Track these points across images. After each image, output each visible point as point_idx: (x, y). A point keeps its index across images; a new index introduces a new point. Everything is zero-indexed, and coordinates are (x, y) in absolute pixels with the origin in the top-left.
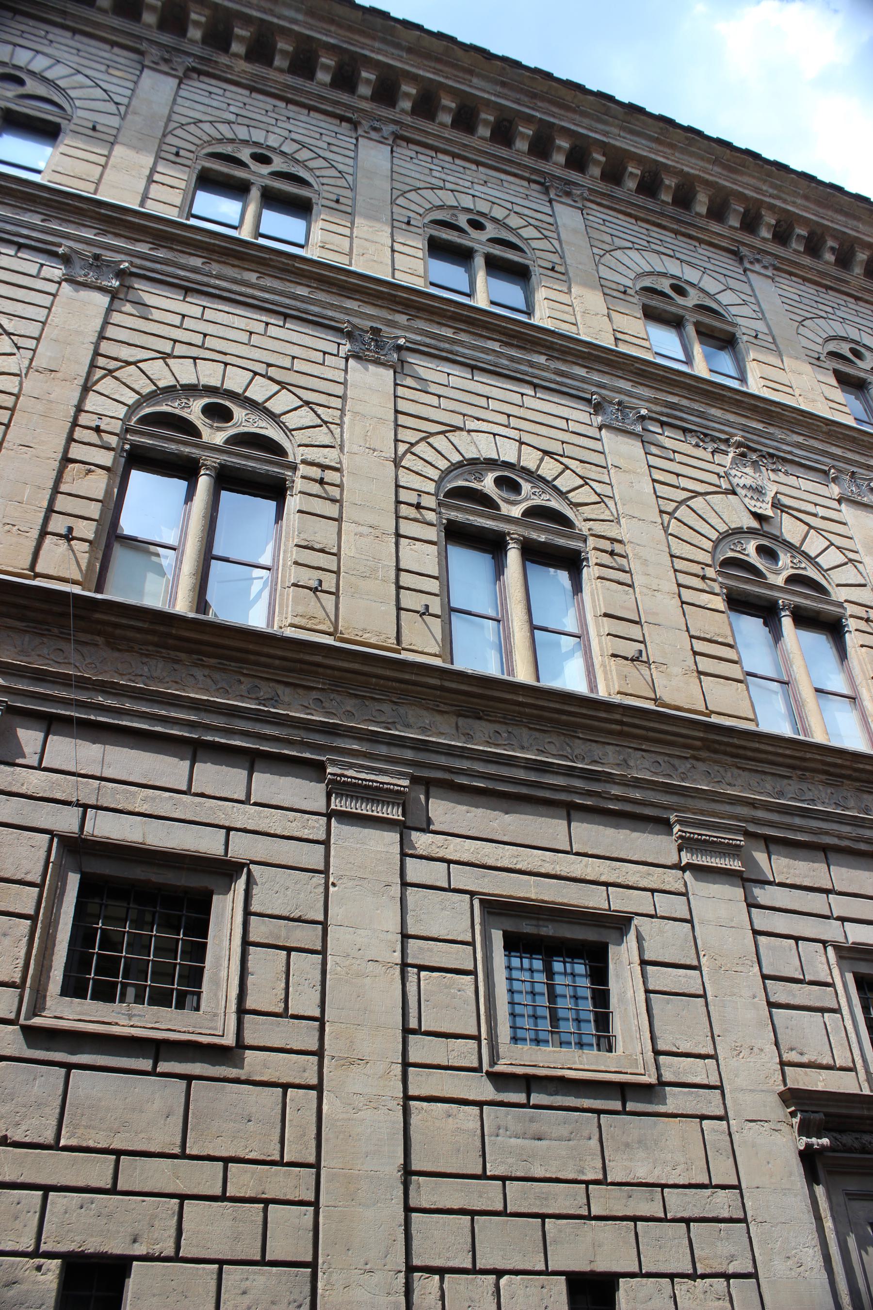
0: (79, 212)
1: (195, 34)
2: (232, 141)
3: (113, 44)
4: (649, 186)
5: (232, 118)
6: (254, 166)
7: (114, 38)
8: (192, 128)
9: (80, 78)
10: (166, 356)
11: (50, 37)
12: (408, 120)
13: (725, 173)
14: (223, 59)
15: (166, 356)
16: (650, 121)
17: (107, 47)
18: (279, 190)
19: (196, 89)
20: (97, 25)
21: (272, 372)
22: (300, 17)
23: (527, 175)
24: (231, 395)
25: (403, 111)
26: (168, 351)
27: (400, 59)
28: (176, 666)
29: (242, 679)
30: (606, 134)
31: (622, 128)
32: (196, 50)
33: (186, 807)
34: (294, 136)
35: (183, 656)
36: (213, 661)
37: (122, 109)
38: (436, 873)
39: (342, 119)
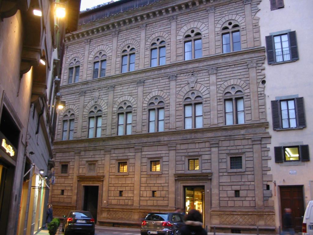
12: (147, 21)
20: (106, 34)
30: (175, 3)
33: (125, 154)
38: (144, 156)
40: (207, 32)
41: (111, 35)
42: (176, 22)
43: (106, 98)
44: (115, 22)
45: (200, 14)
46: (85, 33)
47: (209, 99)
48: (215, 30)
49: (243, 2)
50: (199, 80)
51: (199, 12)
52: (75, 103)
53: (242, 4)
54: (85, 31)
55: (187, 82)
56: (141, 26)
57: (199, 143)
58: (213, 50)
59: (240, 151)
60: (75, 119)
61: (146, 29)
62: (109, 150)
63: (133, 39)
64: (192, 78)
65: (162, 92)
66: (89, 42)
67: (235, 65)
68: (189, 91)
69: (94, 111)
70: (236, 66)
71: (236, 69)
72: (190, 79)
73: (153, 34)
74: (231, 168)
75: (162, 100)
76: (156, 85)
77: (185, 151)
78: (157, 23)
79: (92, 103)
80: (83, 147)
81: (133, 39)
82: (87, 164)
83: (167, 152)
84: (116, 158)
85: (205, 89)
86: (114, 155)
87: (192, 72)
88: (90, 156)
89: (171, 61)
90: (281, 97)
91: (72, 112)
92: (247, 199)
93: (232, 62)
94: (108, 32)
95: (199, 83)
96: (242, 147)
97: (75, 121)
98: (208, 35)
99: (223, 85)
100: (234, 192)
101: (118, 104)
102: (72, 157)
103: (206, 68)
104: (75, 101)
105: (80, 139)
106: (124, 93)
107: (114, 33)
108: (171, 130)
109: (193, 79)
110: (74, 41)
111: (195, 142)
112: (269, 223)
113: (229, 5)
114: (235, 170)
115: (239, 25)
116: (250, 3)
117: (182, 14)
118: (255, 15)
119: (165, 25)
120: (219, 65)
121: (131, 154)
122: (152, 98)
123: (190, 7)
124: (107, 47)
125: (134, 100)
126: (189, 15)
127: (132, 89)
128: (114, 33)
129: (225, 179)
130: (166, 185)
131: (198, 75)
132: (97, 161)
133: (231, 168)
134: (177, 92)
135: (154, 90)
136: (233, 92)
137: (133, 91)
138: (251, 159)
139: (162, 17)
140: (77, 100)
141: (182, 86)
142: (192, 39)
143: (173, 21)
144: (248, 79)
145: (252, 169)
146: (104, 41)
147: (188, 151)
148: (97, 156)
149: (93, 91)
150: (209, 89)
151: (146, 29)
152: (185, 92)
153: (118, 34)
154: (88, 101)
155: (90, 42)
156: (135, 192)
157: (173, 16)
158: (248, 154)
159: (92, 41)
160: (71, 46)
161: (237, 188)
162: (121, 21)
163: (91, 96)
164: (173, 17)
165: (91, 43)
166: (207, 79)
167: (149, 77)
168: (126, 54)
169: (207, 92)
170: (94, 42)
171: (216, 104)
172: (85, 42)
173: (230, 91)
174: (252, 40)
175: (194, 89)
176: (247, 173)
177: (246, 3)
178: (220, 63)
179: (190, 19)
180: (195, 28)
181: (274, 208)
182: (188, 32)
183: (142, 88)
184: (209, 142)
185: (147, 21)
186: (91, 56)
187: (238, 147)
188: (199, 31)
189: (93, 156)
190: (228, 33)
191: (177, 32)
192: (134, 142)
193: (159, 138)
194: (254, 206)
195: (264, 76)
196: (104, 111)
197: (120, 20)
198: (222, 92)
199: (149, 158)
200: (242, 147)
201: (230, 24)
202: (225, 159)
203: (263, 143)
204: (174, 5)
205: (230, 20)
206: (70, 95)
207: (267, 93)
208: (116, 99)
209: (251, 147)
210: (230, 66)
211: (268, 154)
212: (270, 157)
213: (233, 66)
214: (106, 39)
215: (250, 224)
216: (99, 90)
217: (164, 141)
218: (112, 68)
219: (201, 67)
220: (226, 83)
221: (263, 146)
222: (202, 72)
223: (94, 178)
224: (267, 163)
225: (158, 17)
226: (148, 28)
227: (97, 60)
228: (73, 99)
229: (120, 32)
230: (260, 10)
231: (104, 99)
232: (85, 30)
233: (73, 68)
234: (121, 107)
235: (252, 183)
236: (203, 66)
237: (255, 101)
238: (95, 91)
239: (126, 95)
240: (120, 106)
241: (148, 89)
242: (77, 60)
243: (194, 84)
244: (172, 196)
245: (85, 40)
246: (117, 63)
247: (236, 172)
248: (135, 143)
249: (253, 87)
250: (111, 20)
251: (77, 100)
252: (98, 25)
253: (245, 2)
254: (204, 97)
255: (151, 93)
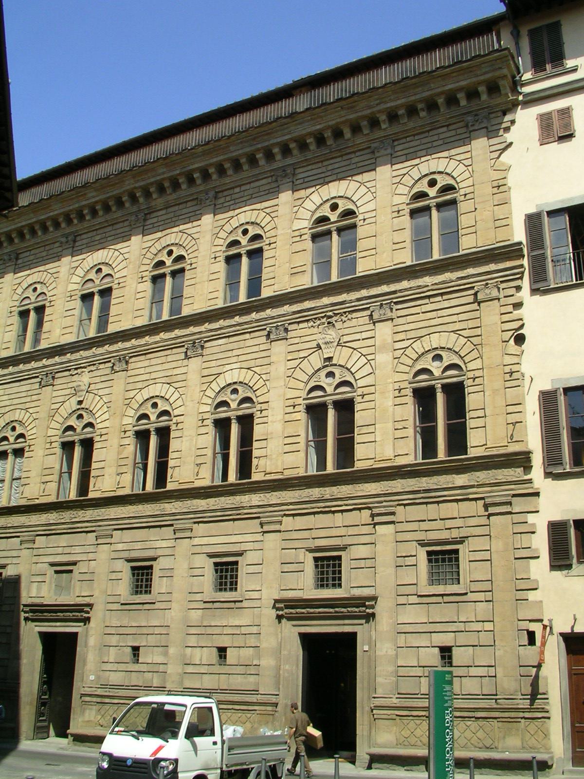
4: (320, 140)
13: (349, 111)
16: (303, 114)
23: (269, 175)
31: (296, 125)
33: (148, 545)
40: (371, 206)
41: (126, 223)
42: (293, 182)
43: (107, 391)
44: (135, 188)
45: (356, 160)
46: (61, 220)
47: (372, 389)
48: (392, 201)
49: (467, 126)
50: (346, 339)
51: (353, 156)
52: (28, 405)
53: (464, 130)
54: (61, 214)
55: (314, 344)
56: (202, 196)
57: (342, 511)
58: (385, 255)
59: (455, 534)
60: (27, 449)
61: (215, 205)
62: (109, 532)
63: (180, 231)
64: (330, 332)
65: (251, 373)
66: (72, 243)
67: (442, 294)
68: (319, 370)
69: (75, 427)
70: (445, 297)
71: (446, 304)
72: (324, 336)
73: (233, 217)
74: (431, 582)
75: (249, 395)
76: (235, 353)
77: (306, 534)
78: (243, 188)
79: (72, 404)
80: (42, 525)
81: (180, 231)
83: (259, 537)
84: (126, 555)
85: (363, 360)
86: (120, 547)
87: (330, 317)
88: (60, 550)
89: (276, 287)
90: (568, 379)
91: (19, 430)
92: (473, 671)
93: (436, 287)
94: (119, 214)
95: (347, 344)
96: (459, 523)
97: (26, 455)
98: (373, 214)
99: (409, 351)
100: (437, 650)
101: (136, 406)
102: (14, 553)
103: (367, 304)
104: (28, 399)
105: (37, 502)
106: (154, 376)
107: (133, 218)
108: (268, 477)
109: (332, 335)
110: (33, 241)
111: (333, 509)
112: (532, 742)
113: (431, 133)
114: (440, 589)
115: (456, 186)
116: (486, 128)
117: (308, 162)
118: (498, 158)
119: (263, 193)
120: (399, 294)
121: (164, 544)
122: (224, 388)
123: (328, 143)
124: (117, 253)
125: (177, 395)
126: (325, 163)
127: (174, 365)
128: (133, 218)
129: (413, 615)
130: (255, 630)
131: (346, 325)
132: (74, 563)
133: (431, 582)
134: (289, 373)
135: (228, 367)
136: (436, 368)
137: (176, 372)
138: (486, 556)
139: (256, 171)
140: (34, 398)
141: (302, 354)
142: (333, 227)
143: (284, 181)
144: (478, 332)
145: (486, 586)
146: (109, 239)
147: (315, 533)
148: (78, 550)
149: (76, 372)
150: (372, 362)
151: (215, 205)
152: (310, 371)
153: (145, 220)
154: (61, 399)
155: (75, 241)
156: (172, 650)
157: (283, 169)
158: (473, 543)
159: (78, 238)
160: (28, 253)
161: (446, 640)
162: (152, 184)
163: (70, 385)
164: (284, 171)
165: (77, 244)
166: (369, 334)
167: (219, 332)
168: (161, 271)
169: (367, 369)
170: (85, 241)
171: (390, 403)
172: (61, 243)
173: (429, 367)
174: (491, 224)
175: (334, 362)
176: (471, 597)
177: (476, 128)
178: (400, 291)
179: (329, 173)
180: (340, 197)
181: (547, 699)
182: (322, 208)
183: (200, 363)
184: (369, 508)
185: (218, 183)
186: (76, 279)
187: (449, 524)
188: (351, 206)
189: (67, 550)
190: (427, 209)
191: (295, 209)
192: (174, 511)
193: (238, 498)
194: (495, 693)
195: (520, 323)
196: (100, 426)
197: (149, 181)
198: (407, 369)
199: (211, 556)
200: (459, 523)
201: (432, 183)
202: (411, 556)
203: (516, 509)
204: (287, 137)
205: (434, 173)
206: (18, 384)
207: (527, 368)
208: (131, 394)
209: (484, 521)
210: (429, 297)
211: (531, 544)
212: (537, 550)
213: (439, 298)
214: (113, 233)
215: (481, 745)
216: (92, 368)
217: (251, 507)
218: (131, 308)
219: (351, 301)
220: (417, 346)
221: (517, 518)
222: (354, 315)
224: (527, 569)
225: (247, 171)
226: (222, 200)
227: (90, 288)
228: (24, 394)
229: (150, 213)
230: (511, 144)
231: (101, 392)
232: (62, 211)
233: (28, 311)
234: (145, 416)
235: (489, 626)
236: (359, 300)
237: (495, 392)
238: (79, 371)
239: (157, 381)
240: (141, 412)
241: (213, 364)
242: (39, 291)
243: (333, 349)
244: (267, 662)
245: (63, 236)
246: (139, 296)
247: (442, 595)
248: (174, 514)
249: (493, 354)
250: (127, 182)
251: (34, 398)
252: (94, 197)
253: (472, 125)
254: (361, 383)
255: (223, 374)
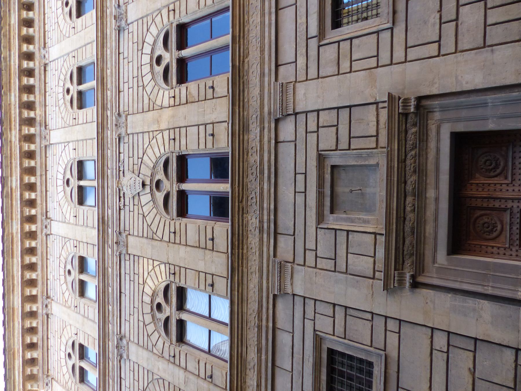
0: (103, 139)
1: (32, 130)
2: (65, 104)
3: (46, 157)
5: (57, 108)
6: (71, 92)
7: (44, 157)
8: (65, 119)
9: (60, 162)
10: (144, 87)
11: (51, 177)
12: (37, 46)
14: (38, 119)
15: (144, 87)
17: (48, 159)
18: (77, 80)
19: (51, 124)
20: (41, 163)
21: (140, 48)
22: (13, 94)
24: (151, 58)
25: (34, 48)
26: (142, 87)
27: (14, 53)
28: (251, 29)
29: (250, 3)
32: (38, 128)
34: (57, 84)
35: (246, 29)
36: (246, 17)
37: (66, 144)
39: (45, 70)
69: (165, 192)
82: (331, 221)
88: (300, 199)
223: (402, 161)
